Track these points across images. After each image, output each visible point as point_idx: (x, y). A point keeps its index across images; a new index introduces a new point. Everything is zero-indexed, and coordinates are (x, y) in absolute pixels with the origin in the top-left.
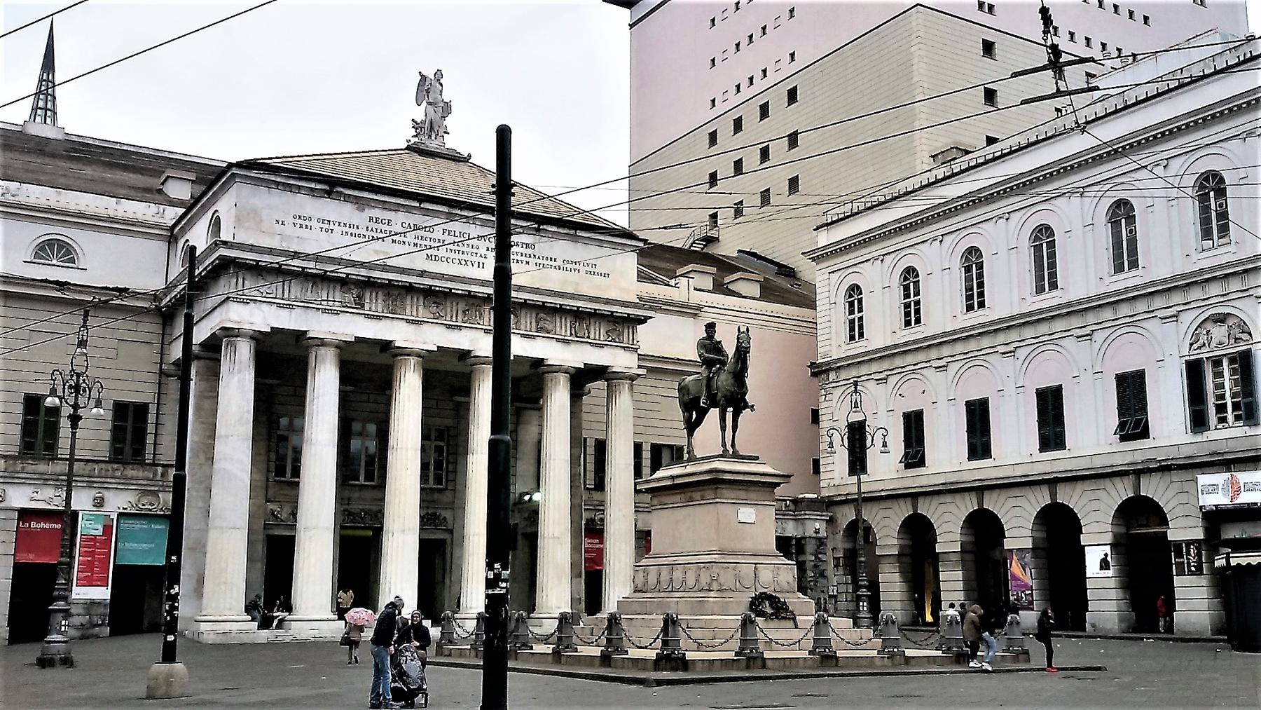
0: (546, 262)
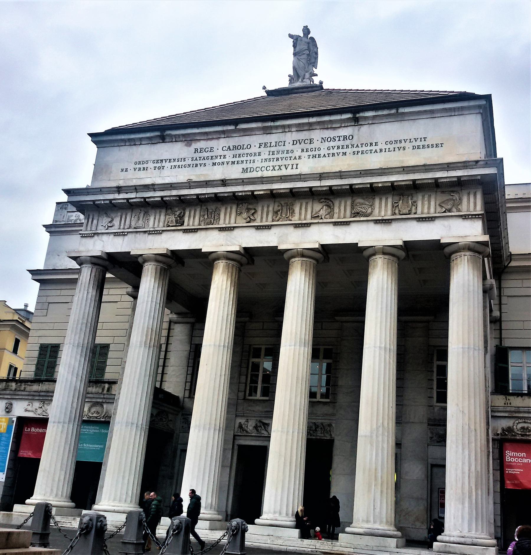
0: (364, 148)
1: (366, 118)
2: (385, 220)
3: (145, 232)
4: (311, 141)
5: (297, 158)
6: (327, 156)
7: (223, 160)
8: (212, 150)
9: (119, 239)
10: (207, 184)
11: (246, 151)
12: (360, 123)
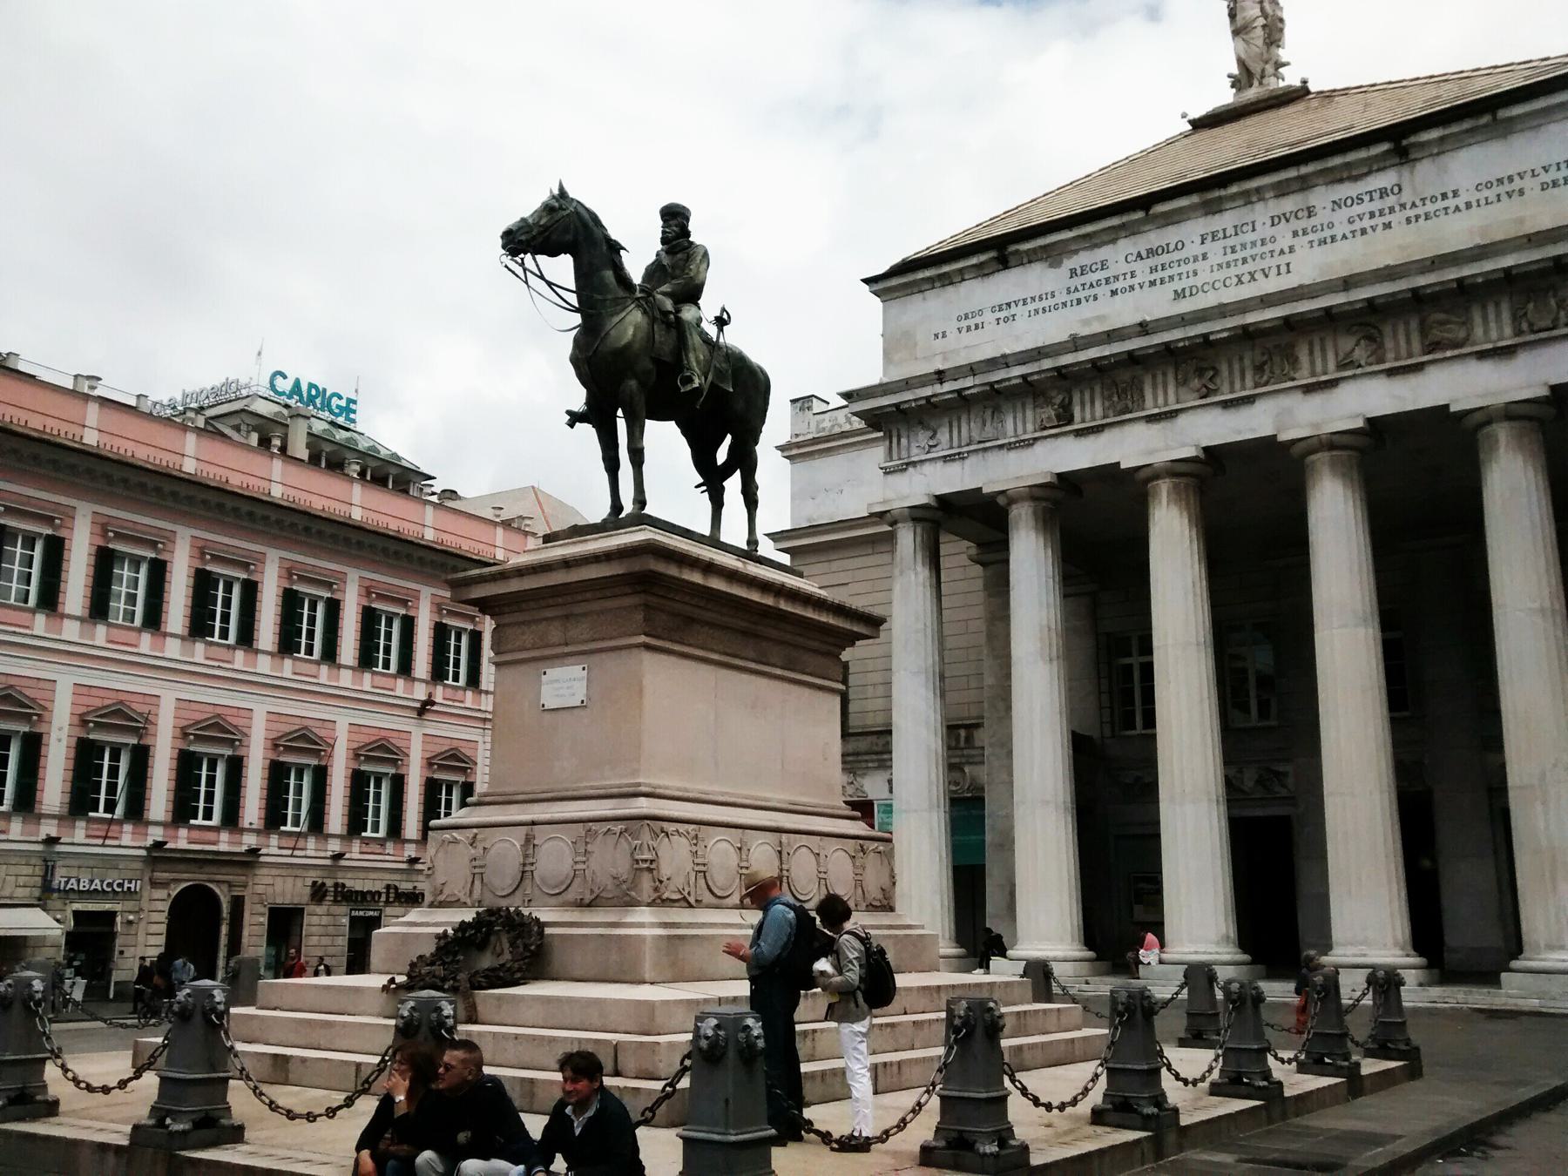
0: (1430, 207)
1: (1422, 145)
2: (1502, 348)
3: (1001, 447)
4: (1310, 212)
5: (1287, 250)
6: (1349, 235)
7: (1130, 281)
8: (1104, 265)
9: (955, 467)
10: (1110, 336)
11: (1176, 256)
12: (1412, 156)
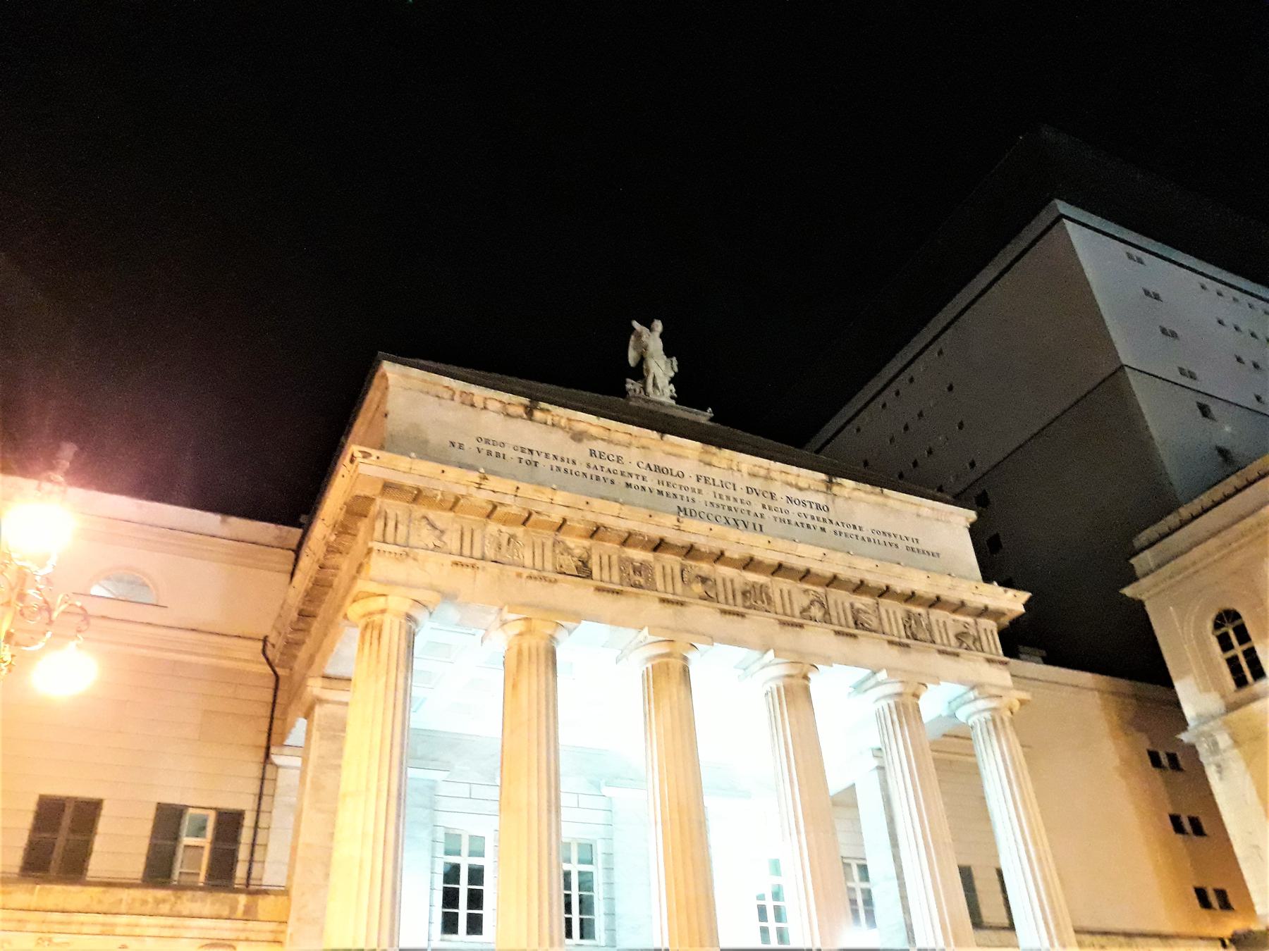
7: (640, 483)
8: (619, 459)
11: (677, 481)
